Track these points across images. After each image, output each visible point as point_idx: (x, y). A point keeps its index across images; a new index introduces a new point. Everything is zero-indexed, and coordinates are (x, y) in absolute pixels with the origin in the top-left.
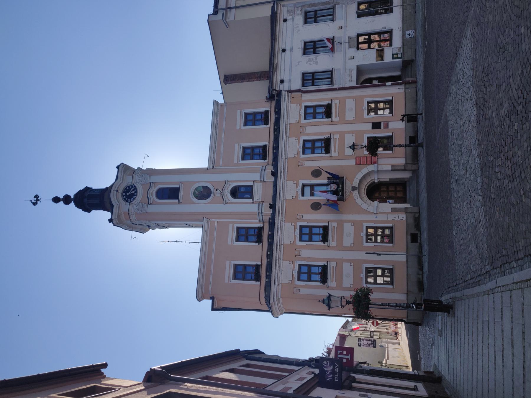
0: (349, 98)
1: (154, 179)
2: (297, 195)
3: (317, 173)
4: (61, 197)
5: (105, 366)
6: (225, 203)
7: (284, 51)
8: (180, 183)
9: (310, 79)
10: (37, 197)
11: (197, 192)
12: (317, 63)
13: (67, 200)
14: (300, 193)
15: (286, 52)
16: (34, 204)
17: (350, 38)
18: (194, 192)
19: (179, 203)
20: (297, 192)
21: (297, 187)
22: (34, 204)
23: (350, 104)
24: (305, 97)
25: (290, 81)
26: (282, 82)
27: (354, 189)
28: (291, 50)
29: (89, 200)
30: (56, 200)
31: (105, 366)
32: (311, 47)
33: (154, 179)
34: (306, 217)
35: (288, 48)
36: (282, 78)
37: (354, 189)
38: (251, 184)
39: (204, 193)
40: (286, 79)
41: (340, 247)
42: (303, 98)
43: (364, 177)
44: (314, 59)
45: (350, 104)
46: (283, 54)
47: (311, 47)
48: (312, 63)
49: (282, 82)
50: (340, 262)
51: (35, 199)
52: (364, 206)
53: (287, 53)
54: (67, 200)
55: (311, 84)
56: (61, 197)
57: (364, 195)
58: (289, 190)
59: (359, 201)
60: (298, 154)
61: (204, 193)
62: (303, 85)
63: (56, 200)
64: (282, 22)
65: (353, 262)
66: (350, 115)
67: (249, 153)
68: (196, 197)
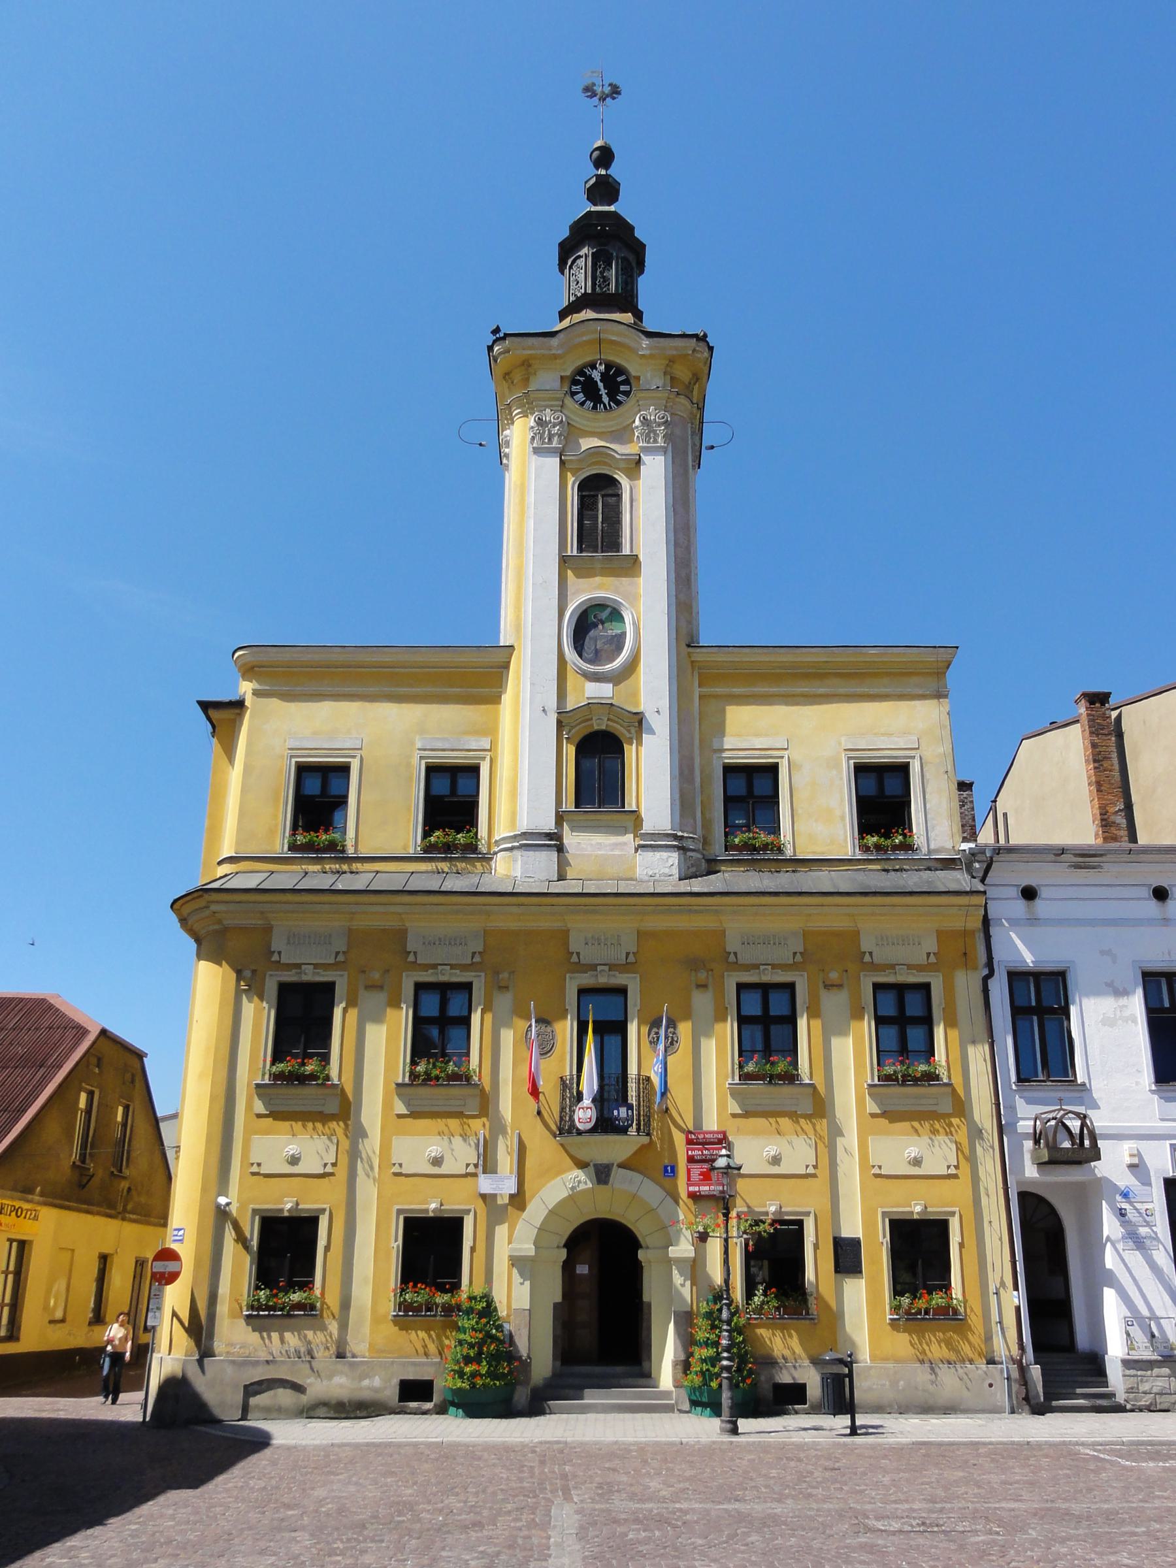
4: (615, 171)
7: (1160, 894)
10: (615, 91)
13: (605, 190)
14: (587, 980)
15: (1153, 903)
19: (564, 561)
20: (593, 967)
21: (612, 967)
22: (589, 91)
24: (966, 983)
25: (1033, 921)
26: (1029, 894)
36: (1044, 893)
38: (631, 804)
40: (1041, 906)
44: (1127, 1013)
46: (1147, 893)
51: (607, 90)
54: (605, 190)
55: (1020, 1002)
56: (615, 171)
60: (737, 966)
62: (1016, 977)
63: (604, 157)
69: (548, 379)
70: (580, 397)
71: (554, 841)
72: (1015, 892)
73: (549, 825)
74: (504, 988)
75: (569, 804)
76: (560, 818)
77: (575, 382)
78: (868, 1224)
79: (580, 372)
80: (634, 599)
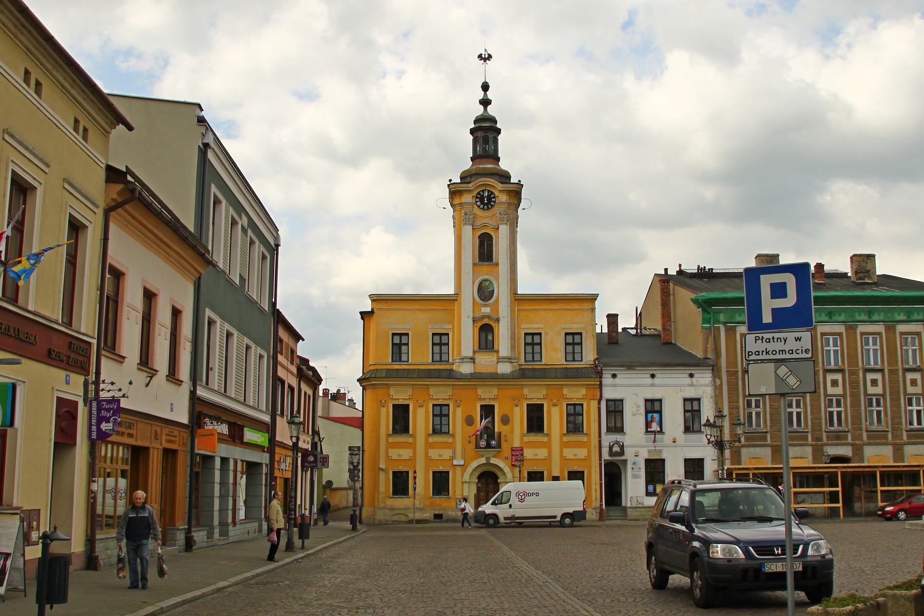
0: (589, 452)
1: (504, 229)
2: (481, 399)
3: (506, 420)
5: (303, 340)
6: (474, 321)
7: (653, 376)
8: (497, 264)
9: (616, 409)
11: (487, 283)
12: (634, 415)
13: (485, 102)
16: (480, 56)
17: (660, 451)
18: (487, 280)
19: (474, 265)
23: (582, 453)
24: (594, 404)
25: (615, 385)
26: (614, 376)
27: (488, 459)
28: (652, 385)
29: (486, 132)
30: (485, 87)
31: (303, 340)
32: (653, 407)
33: (504, 229)
34: (459, 411)
35: (656, 381)
37: (488, 459)
38: (496, 348)
39: (485, 293)
40: (617, 381)
41: (429, 446)
42: (592, 402)
43: (501, 469)
45: (582, 453)
46: (648, 376)
47: (653, 407)
48: (635, 409)
49: (614, 376)
50: (413, 446)
52: (470, 470)
53: (650, 381)
54: (485, 102)
57: (484, 469)
58: (487, 394)
59: (475, 464)
61: (485, 293)
63: (485, 87)
64: (690, 372)
65: (413, 459)
66: (569, 453)
67: (533, 341)
68: (481, 284)
69: (468, 198)
70: (479, 203)
71: (473, 360)
72: (610, 376)
73: (471, 354)
74: (459, 406)
75: (476, 348)
76: (474, 352)
77: (477, 198)
78: (562, 471)
79: (479, 193)
80: (497, 278)
